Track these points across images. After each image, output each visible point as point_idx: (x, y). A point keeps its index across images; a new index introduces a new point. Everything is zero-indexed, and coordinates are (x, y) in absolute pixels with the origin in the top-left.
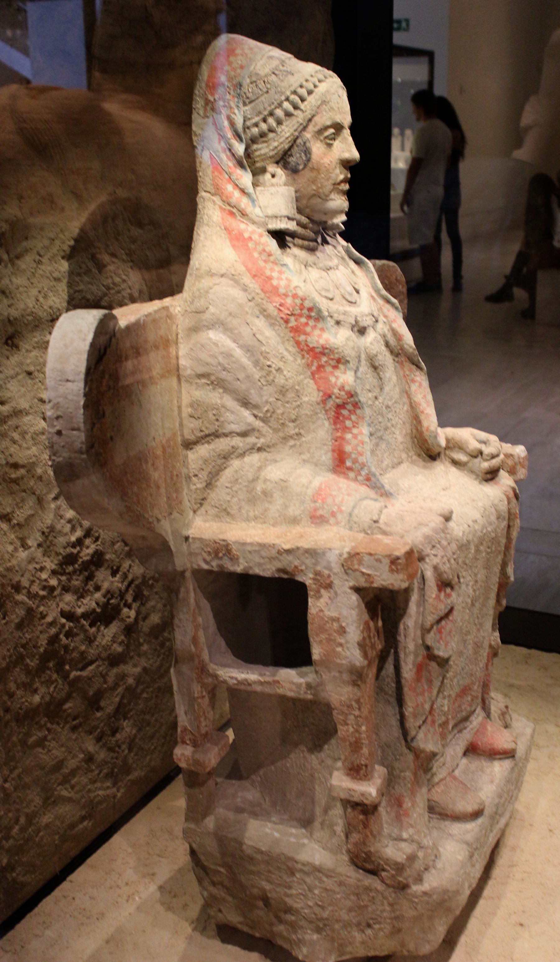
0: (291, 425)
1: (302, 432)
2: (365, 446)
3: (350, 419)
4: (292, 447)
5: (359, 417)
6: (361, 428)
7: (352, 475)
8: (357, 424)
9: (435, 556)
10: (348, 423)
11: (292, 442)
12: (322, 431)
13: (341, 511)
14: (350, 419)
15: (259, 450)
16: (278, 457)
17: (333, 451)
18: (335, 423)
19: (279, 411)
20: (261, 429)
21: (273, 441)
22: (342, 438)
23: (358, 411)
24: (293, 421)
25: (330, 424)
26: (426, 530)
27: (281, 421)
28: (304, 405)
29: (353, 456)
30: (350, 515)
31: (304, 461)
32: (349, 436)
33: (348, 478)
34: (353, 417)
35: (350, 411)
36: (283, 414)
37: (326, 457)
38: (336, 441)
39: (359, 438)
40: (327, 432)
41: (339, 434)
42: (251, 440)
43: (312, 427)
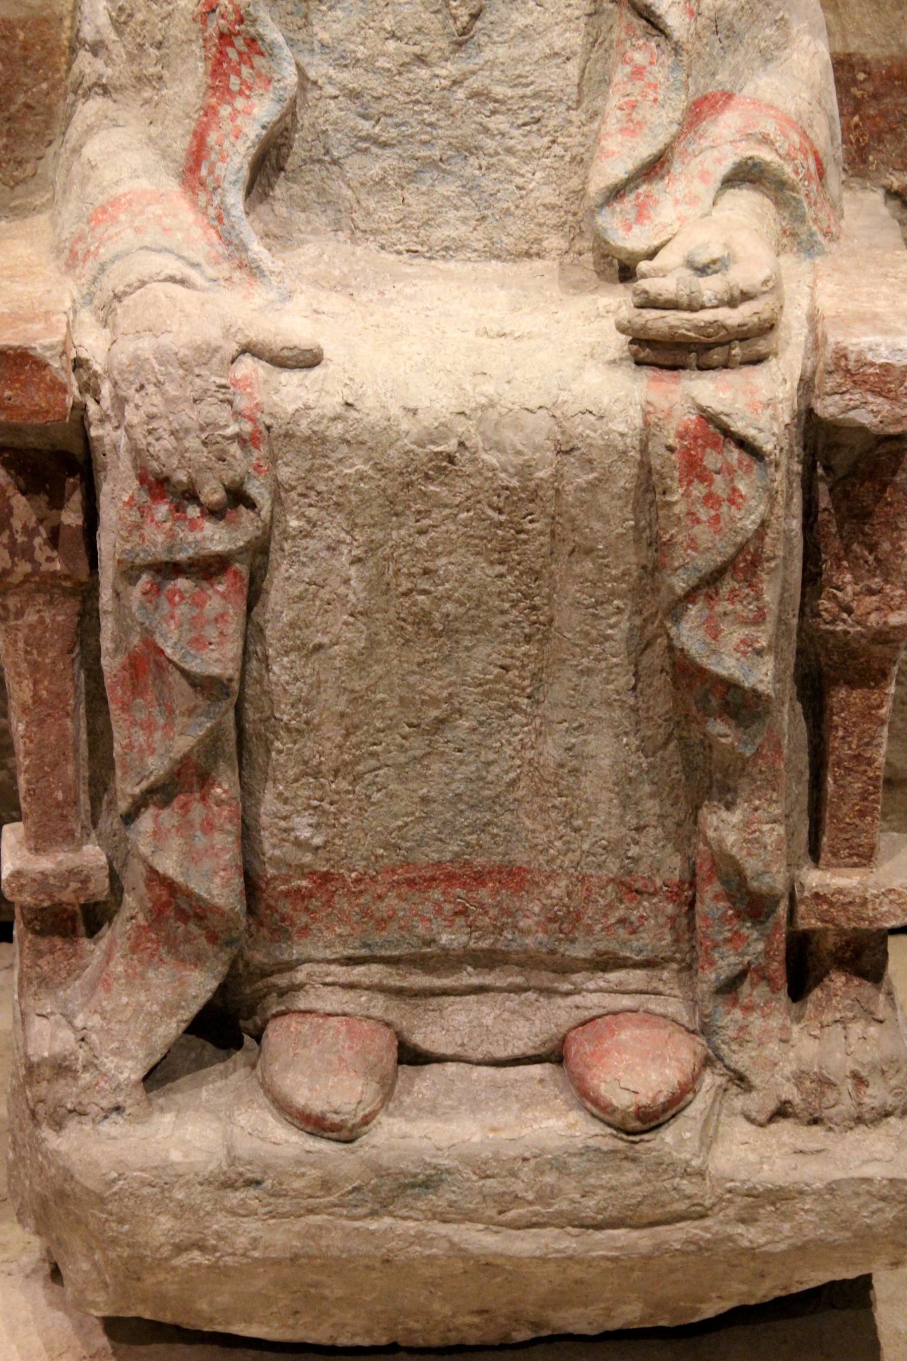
0: (153, 51)
1: (166, 74)
2: (240, 142)
3: (238, 73)
4: (147, 102)
5: (259, 75)
6: (255, 100)
7: (203, 198)
8: (250, 88)
9: (137, 407)
10: (234, 82)
11: (147, 93)
12: (188, 83)
13: (96, 254)
14: (238, 73)
15: (105, 90)
16: (123, 116)
17: (195, 134)
18: (214, 74)
19: (140, 17)
20: (111, 47)
21: (123, 81)
22: (216, 113)
23: (258, 61)
24: (159, 45)
25: (205, 73)
26: (146, 345)
27: (139, 40)
28: (177, 15)
29: (213, 157)
30: (102, 269)
31: (150, 138)
32: (225, 111)
33: (194, 203)
34: (245, 71)
35: (240, 54)
36: (144, 23)
37: (181, 144)
38: (206, 115)
39: (239, 121)
40: (198, 87)
41: (213, 101)
42: (99, 64)
43: (182, 69)
